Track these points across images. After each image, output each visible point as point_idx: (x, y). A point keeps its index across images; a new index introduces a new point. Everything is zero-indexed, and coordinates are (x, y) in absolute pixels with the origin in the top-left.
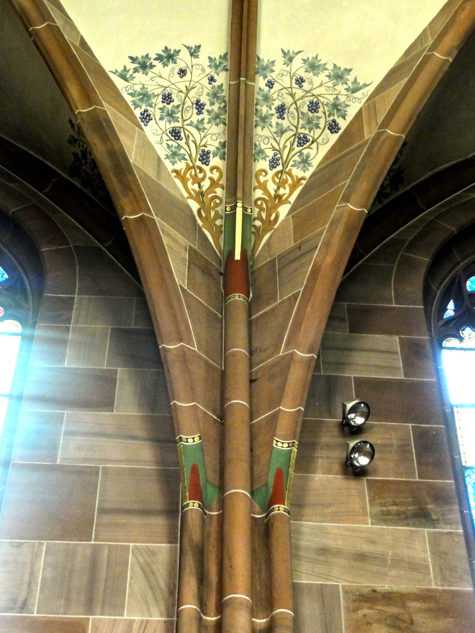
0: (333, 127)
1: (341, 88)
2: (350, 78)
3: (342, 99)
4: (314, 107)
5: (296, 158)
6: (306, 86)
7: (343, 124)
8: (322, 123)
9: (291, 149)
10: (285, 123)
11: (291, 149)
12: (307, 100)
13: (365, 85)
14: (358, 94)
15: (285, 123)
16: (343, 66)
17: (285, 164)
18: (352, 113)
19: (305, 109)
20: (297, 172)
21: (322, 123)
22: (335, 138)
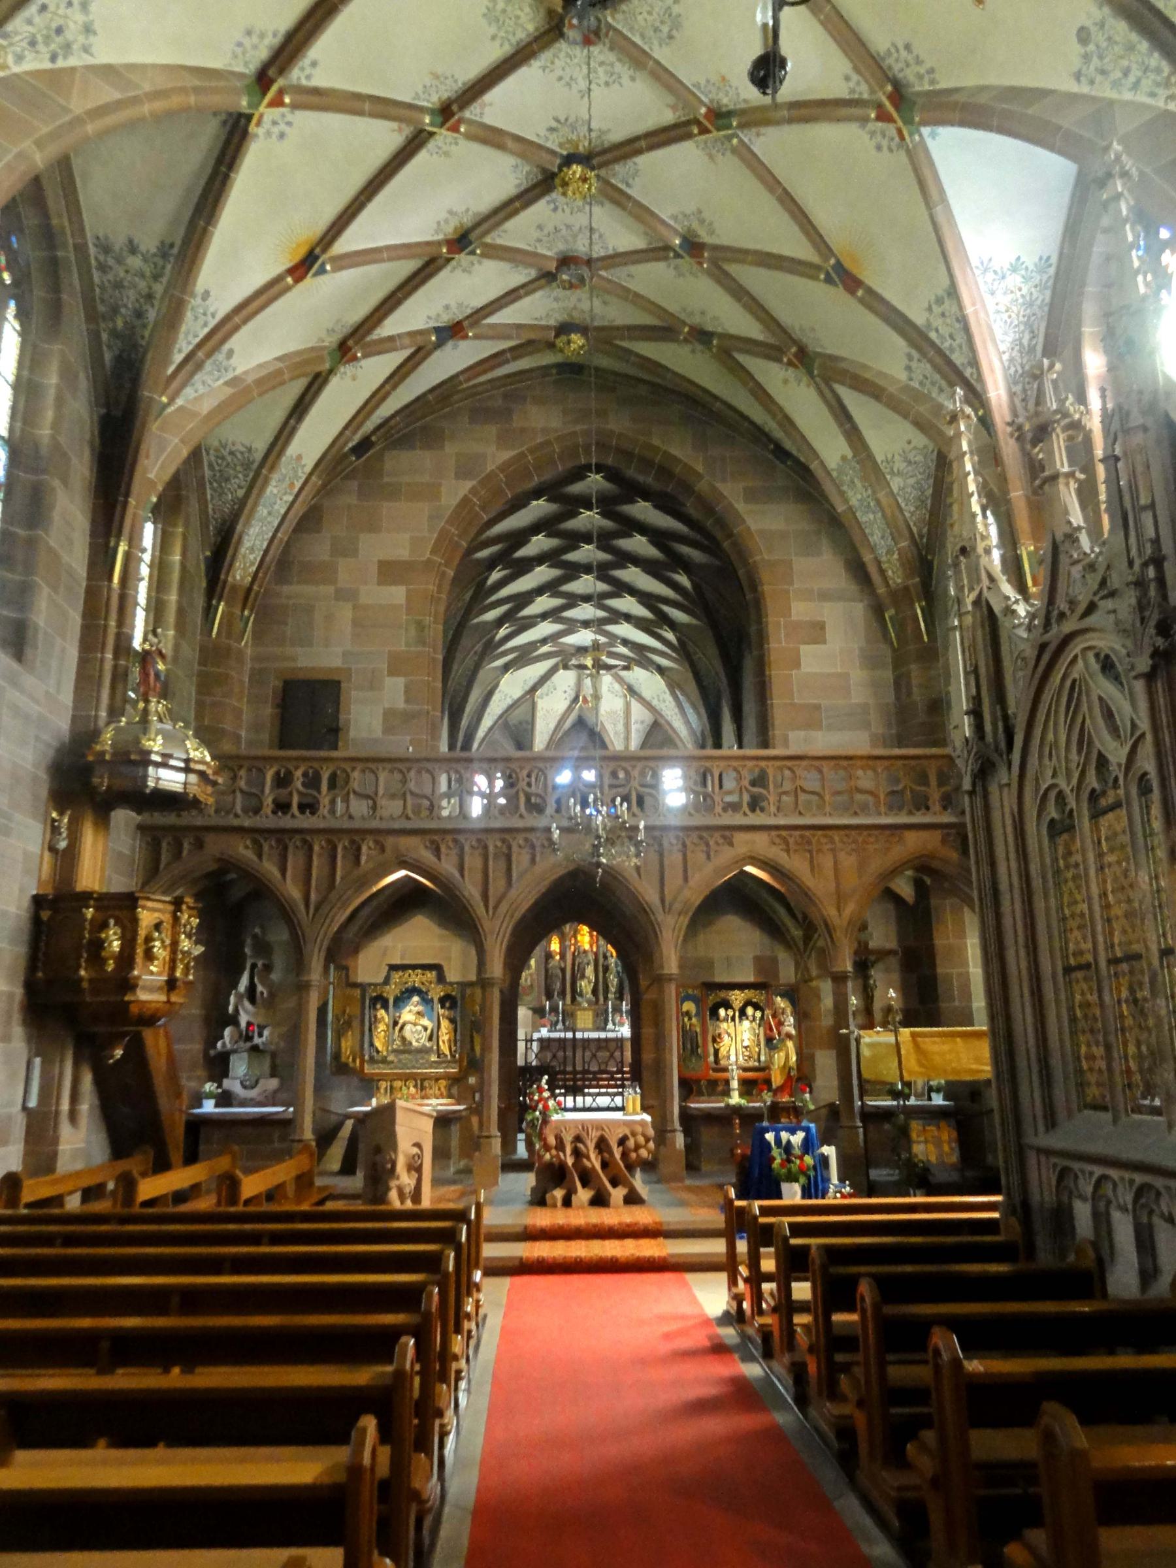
0: (53, 58)
1: (81, 39)
2: (92, 39)
3: (75, 47)
4: (59, 31)
5: (19, 49)
6: (69, 11)
7: (61, 63)
8: (53, 46)
9: (22, 40)
10: (37, 20)
11: (22, 40)
12: (61, 22)
13: (92, 55)
14: (85, 56)
15: (37, 20)
16: (97, 26)
17: (11, 44)
18: (72, 62)
19: (54, 25)
20: (10, 59)
21: (53, 46)
22: (48, 65)
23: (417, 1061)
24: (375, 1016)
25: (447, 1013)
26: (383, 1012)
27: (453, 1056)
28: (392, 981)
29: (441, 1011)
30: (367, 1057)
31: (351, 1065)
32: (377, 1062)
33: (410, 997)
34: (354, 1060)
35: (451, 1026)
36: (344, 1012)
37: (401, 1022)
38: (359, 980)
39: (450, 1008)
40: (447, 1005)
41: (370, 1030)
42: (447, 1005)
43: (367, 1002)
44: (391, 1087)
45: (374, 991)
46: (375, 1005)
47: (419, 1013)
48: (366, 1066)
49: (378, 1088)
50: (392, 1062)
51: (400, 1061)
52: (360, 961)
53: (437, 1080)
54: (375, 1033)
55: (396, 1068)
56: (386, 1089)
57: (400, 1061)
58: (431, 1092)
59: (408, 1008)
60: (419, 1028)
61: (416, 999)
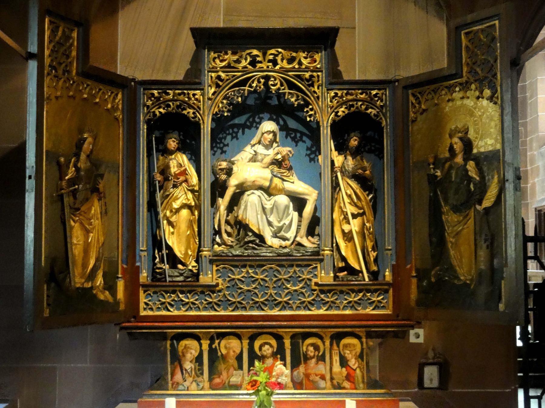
23: (280, 285)
24: (165, 171)
25: (350, 163)
26: (183, 159)
27: (374, 275)
28: (209, 77)
29: (339, 160)
30: (144, 276)
31: (104, 296)
32: (174, 288)
33: (254, 125)
34: (110, 287)
35: (366, 198)
36: (79, 145)
37: (233, 182)
38: (121, 70)
39: (356, 153)
40: (354, 142)
41: (152, 206)
42: (354, 142)
43: (143, 129)
44: (213, 352)
45: (158, 102)
46: (162, 141)
47: (277, 163)
48: (143, 298)
49: (177, 359)
50: (212, 289)
51: (233, 285)
52: (120, 22)
53: (337, 337)
54: (163, 212)
55: (226, 303)
56: (199, 359)
57: (233, 285)
58: (322, 368)
59: (248, 152)
60: (283, 200)
61: (268, 126)
